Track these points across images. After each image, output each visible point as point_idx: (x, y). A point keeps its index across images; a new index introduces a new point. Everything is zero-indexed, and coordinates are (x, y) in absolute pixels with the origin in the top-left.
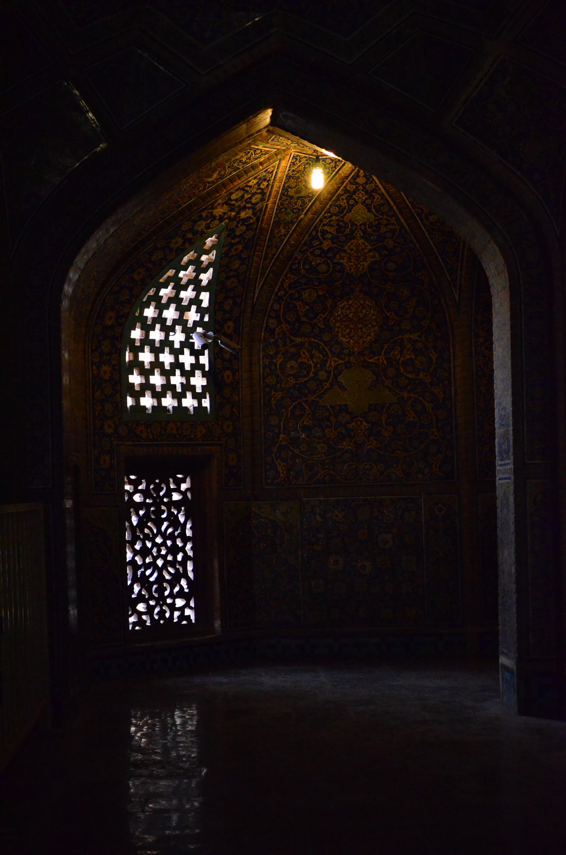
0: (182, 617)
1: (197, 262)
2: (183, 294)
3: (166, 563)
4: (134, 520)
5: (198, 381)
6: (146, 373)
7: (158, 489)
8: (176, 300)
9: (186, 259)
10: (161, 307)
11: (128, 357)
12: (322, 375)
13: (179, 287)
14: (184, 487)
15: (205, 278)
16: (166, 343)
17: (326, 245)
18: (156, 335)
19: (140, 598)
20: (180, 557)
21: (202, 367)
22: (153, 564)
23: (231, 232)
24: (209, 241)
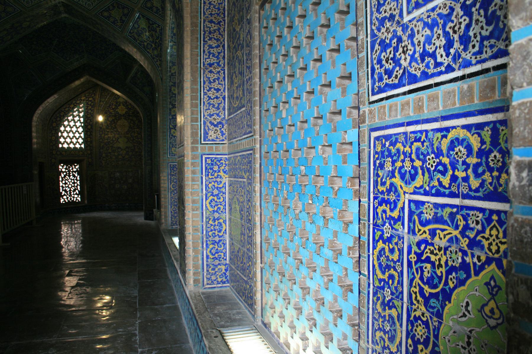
0: (77, 200)
1: (78, 110)
2: (75, 119)
3: (72, 186)
4: (63, 176)
5: (81, 141)
6: (65, 138)
7: (69, 168)
8: (73, 120)
9: (75, 110)
10: (69, 122)
11: (60, 134)
12: (114, 139)
13: (74, 117)
15: (81, 115)
16: (71, 131)
17: (114, 107)
18: (68, 129)
19: (65, 195)
20: (76, 185)
21: (81, 137)
22: (68, 187)
23: (87, 104)
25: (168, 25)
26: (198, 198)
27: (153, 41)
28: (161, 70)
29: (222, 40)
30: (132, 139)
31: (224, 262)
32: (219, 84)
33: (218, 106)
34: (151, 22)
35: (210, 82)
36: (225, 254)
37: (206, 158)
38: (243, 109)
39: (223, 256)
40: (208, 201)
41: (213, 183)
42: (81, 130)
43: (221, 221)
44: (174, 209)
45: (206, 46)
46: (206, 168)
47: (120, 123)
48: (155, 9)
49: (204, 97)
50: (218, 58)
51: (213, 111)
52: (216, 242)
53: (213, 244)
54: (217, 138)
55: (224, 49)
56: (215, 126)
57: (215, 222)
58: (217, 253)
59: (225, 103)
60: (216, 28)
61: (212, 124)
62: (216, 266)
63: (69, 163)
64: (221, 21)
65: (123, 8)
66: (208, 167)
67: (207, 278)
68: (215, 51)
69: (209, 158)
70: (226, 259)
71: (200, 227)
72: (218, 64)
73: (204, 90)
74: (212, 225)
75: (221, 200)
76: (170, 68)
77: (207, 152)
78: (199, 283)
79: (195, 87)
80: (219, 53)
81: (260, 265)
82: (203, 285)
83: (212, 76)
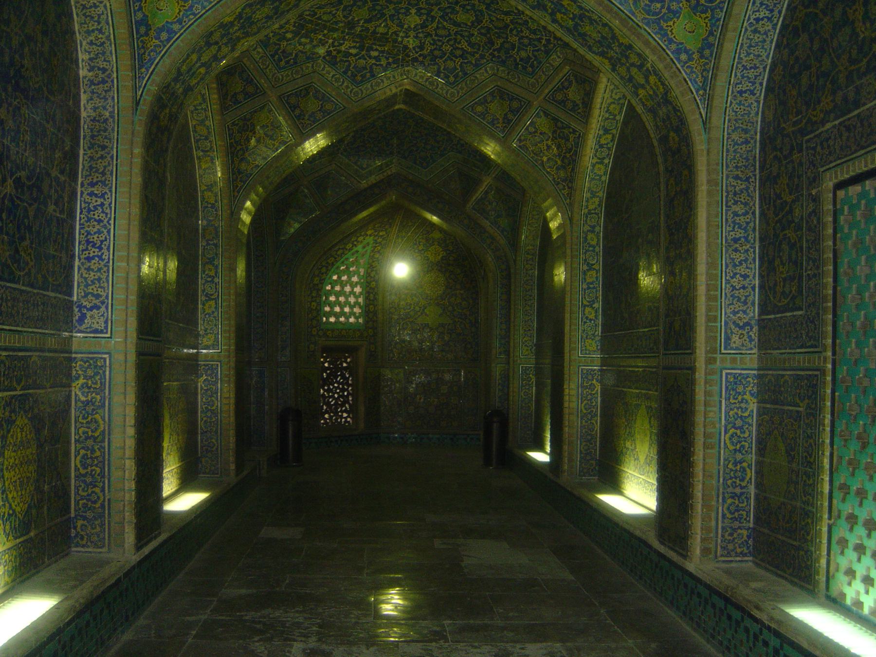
14: (349, 360)
22: (333, 397)
25: (592, 131)
26: (713, 430)
28: (571, 205)
29: (751, 204)
30: (450, 308)
31: (747, 525)
32: (747, 268)
33: (746, 300)
34: (559, 124)
35: (735, 266)
36: (748, 512)
37: (727, 374)
38: (800, 313)
39: (745, 517)
40: (728, 436)
41: (735, 410)
42: (358, 290)
43: (745, 465)
45: (730, 213)
46: (727, 388)
48: (570, 105)
49: (726, 287)
50: (745, 229)
51: (738, 306)
52: (736, 495)
53: (732, 497)
54: (743, 345)
55: (755, 218)
56: (741, 328)
57: (736, 466)
58: (738, 511)
59: (754, 295)
60: (743, 186)
61: (737, 325)
62: (735, 530)
64: (750, 177)
65: (512, 99)
66: (730, 387)
67: (721, 547)
68: (742, 220)
69: (730, 374)
70: (749, 521)
71: (715, 472)
72: (746, 238)
73: (726, 276)
74: (732, 470)
75: (746, 435)
76: (587, 201)
77: (729, 366)
78: (710, 553)
79: (714, 272)
80: (748, 223)
81: (827, 521)
82: (716, 557)
83: (738, 257)
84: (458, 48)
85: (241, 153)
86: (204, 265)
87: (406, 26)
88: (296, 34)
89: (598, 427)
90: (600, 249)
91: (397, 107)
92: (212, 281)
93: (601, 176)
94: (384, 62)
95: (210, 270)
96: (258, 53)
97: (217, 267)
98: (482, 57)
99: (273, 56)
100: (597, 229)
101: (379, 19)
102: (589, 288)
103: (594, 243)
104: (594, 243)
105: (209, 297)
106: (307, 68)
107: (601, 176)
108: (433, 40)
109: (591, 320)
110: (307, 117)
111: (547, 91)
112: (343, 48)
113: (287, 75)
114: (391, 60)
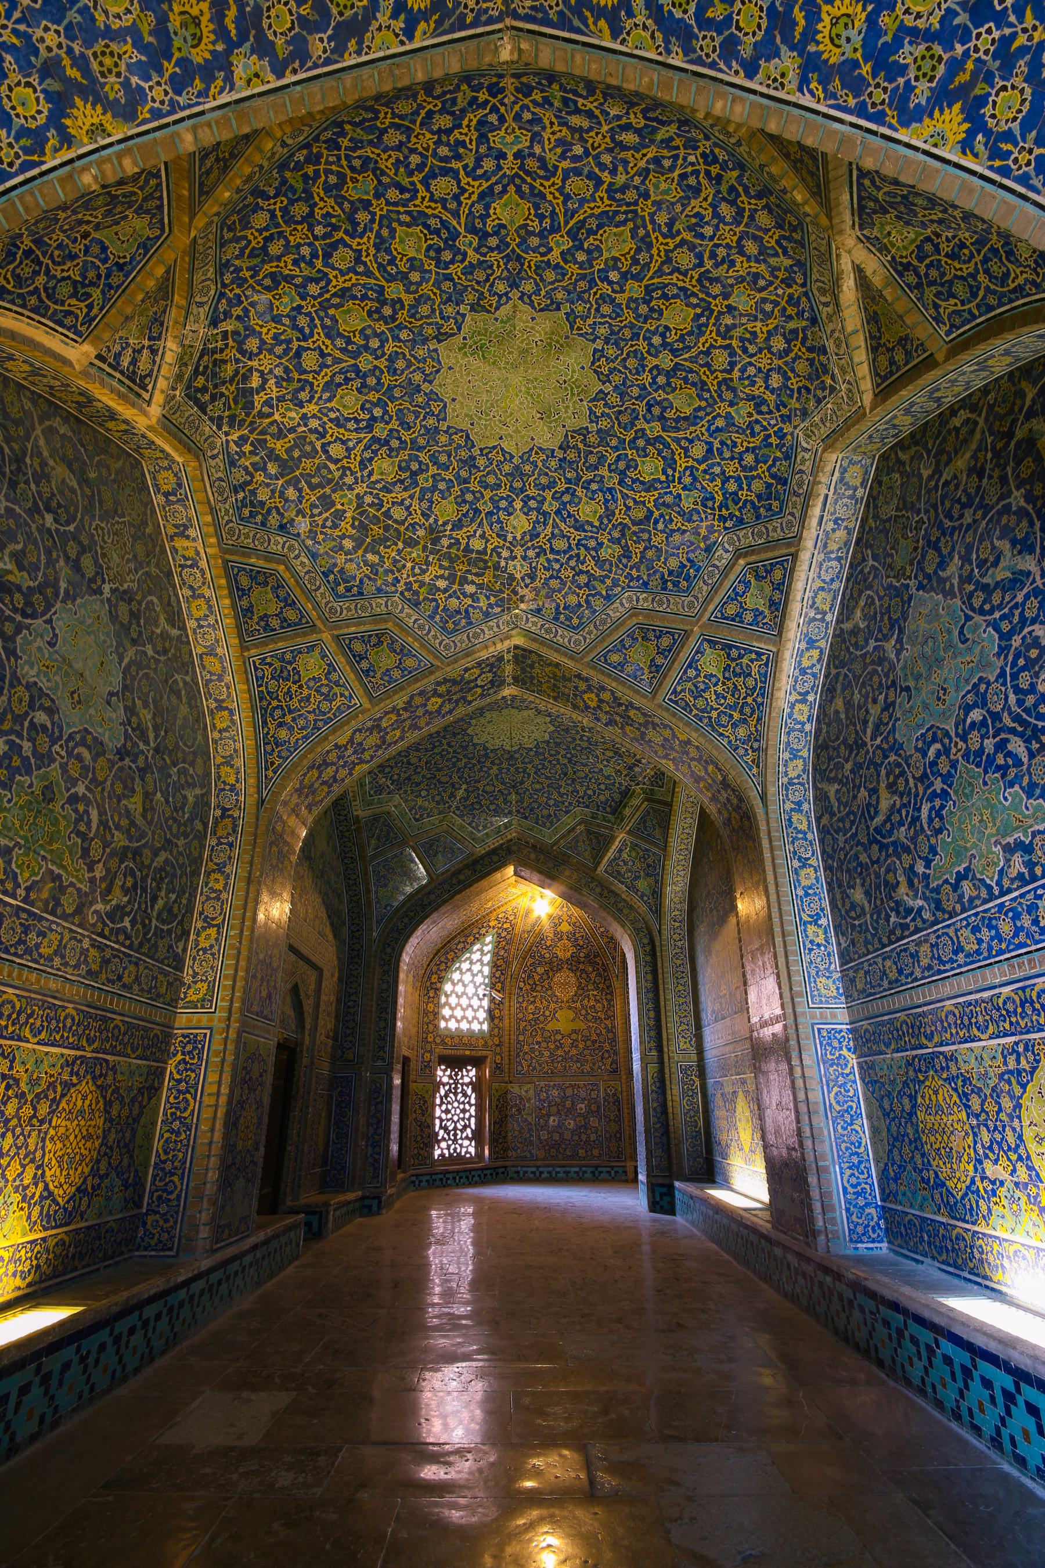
1: (481, 950)
5: (482, 1015)
6: (452, 1009)
11: (443, 999)
15: (487, 959)
18: (459, 989)
23: (499, 935)
24: (488, 939)
25: (790, 645)
27: (736, 704)
44: (854, 1181)
47: (559, 977)
48: (749, 617)
63: (456, 1063)
84: (581, 572)
85: (278, 713)
86: (208, 874)
87: (510, 538)
88: (359, 543)
89: (866, 1138)
90: (814, 835)
91: (507, 692)
92: (218, 898)
93: (803, 724)
94: (483, 604)
95: (217, 880)
96: (302, 564)
97: (228, 877)
98: (615, 584)
99: (325, 574)
100: (805, 807)
101: (472, 521)
102: (807, 894)
103: (804, 827)
104: (804, 827)
105: (208, 922)
106: (379, 605)
107: (803, 724)
108: (548, 560)
109: (819, 945)
110: (378, 675)
111: (711, 607)
112: (427, 579)
113: (349, 609)
114: (492, 600)
